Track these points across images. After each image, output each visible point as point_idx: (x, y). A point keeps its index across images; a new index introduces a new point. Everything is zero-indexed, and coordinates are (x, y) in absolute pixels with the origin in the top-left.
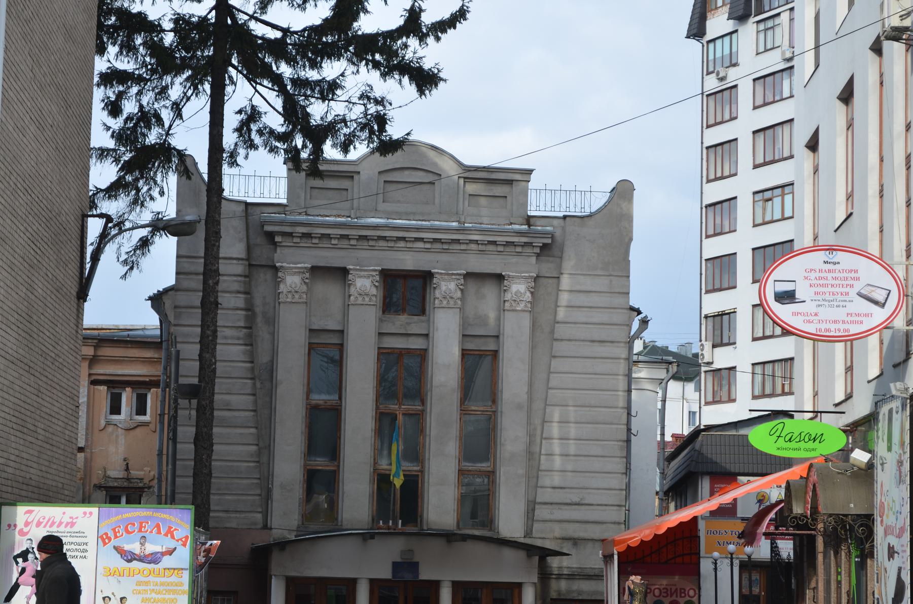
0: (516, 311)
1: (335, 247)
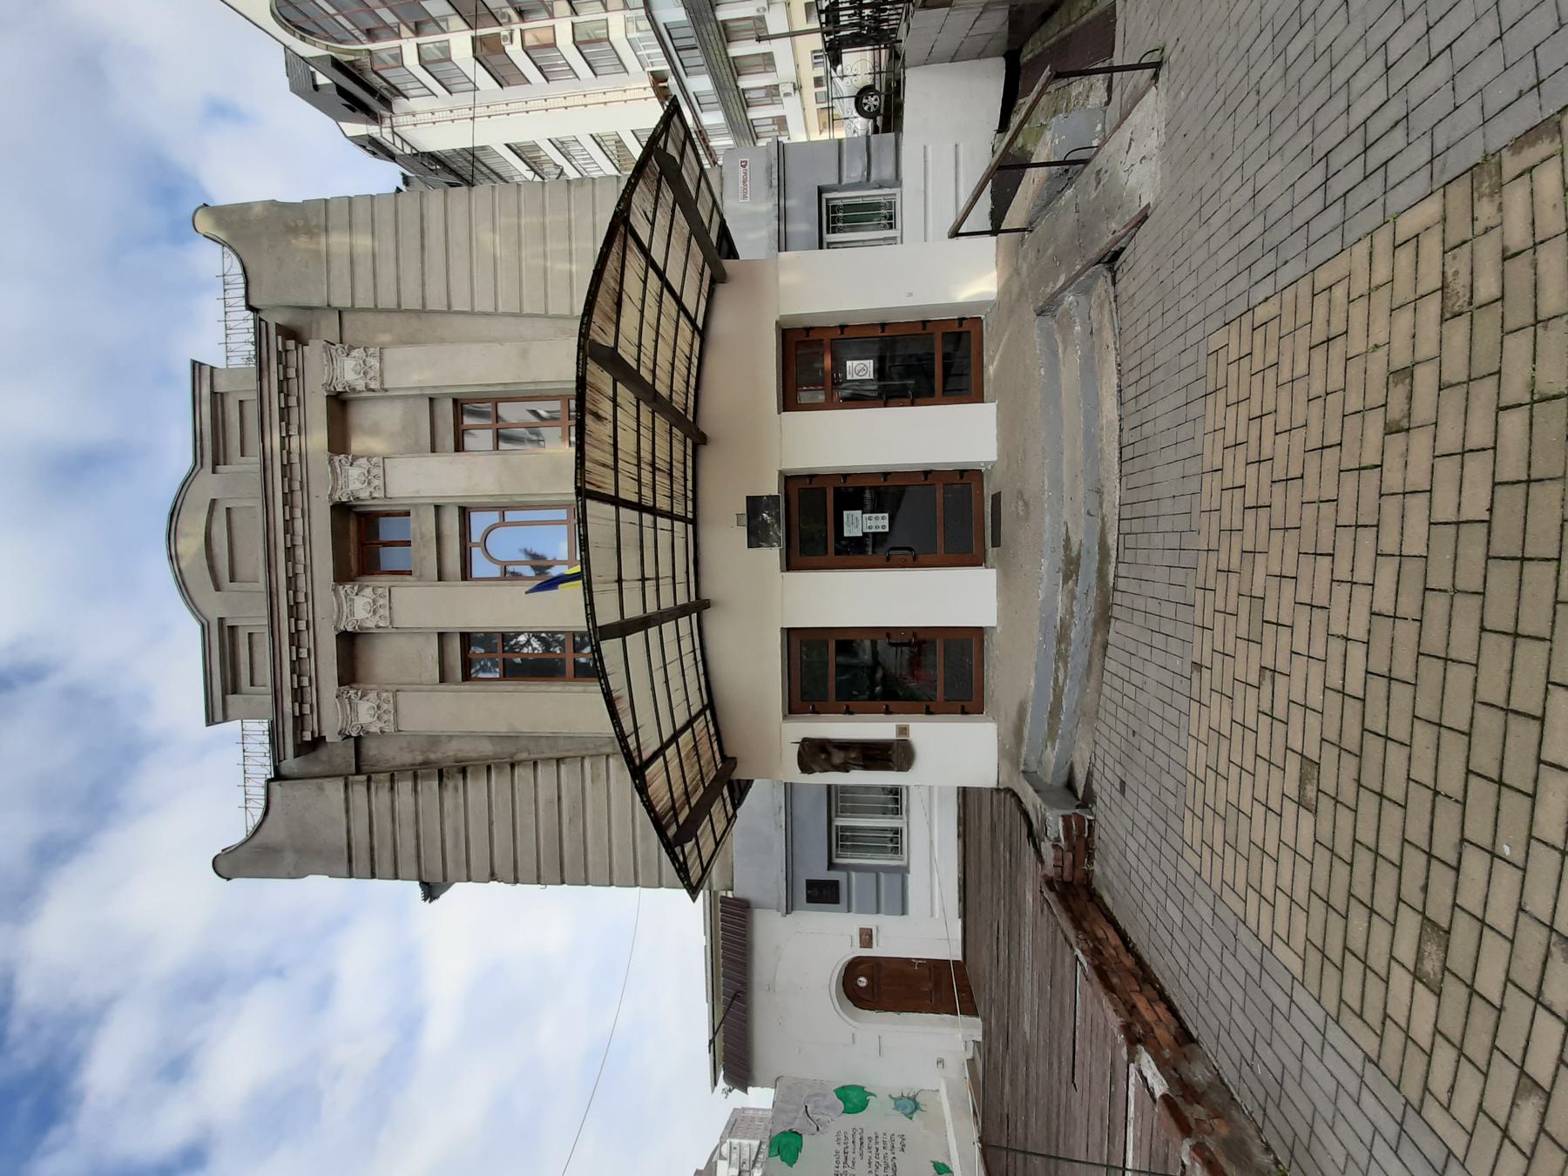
0: (381, 370)
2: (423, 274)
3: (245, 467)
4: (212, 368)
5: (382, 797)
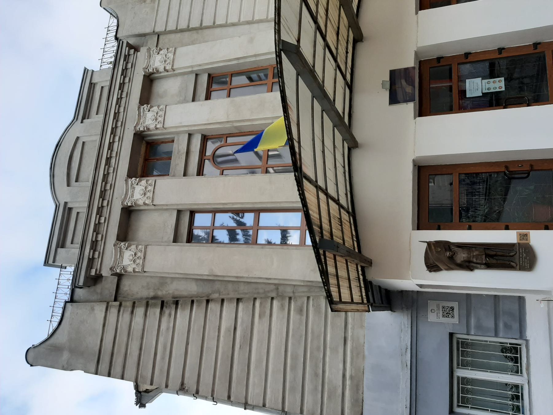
0: (174, 59)
1: (108, 220)
2: (203, 9)
3: (97, 119)
4: (93, 71)
5: (125, 317)
